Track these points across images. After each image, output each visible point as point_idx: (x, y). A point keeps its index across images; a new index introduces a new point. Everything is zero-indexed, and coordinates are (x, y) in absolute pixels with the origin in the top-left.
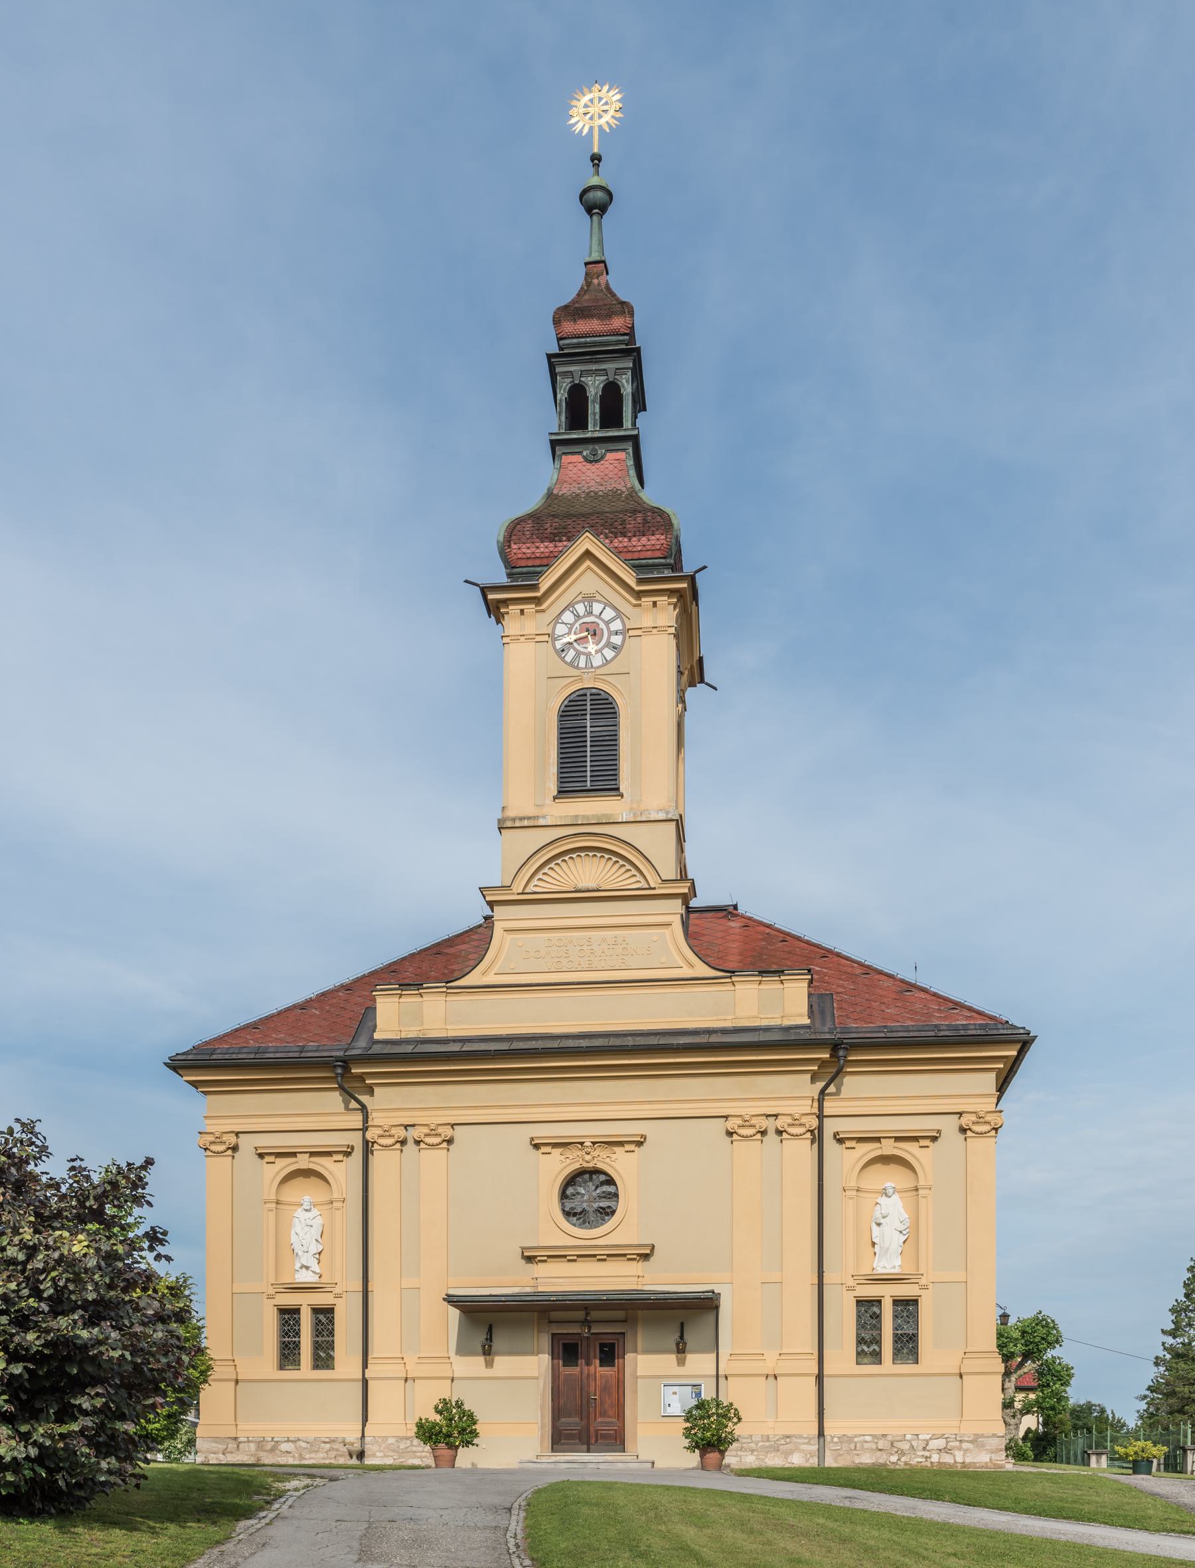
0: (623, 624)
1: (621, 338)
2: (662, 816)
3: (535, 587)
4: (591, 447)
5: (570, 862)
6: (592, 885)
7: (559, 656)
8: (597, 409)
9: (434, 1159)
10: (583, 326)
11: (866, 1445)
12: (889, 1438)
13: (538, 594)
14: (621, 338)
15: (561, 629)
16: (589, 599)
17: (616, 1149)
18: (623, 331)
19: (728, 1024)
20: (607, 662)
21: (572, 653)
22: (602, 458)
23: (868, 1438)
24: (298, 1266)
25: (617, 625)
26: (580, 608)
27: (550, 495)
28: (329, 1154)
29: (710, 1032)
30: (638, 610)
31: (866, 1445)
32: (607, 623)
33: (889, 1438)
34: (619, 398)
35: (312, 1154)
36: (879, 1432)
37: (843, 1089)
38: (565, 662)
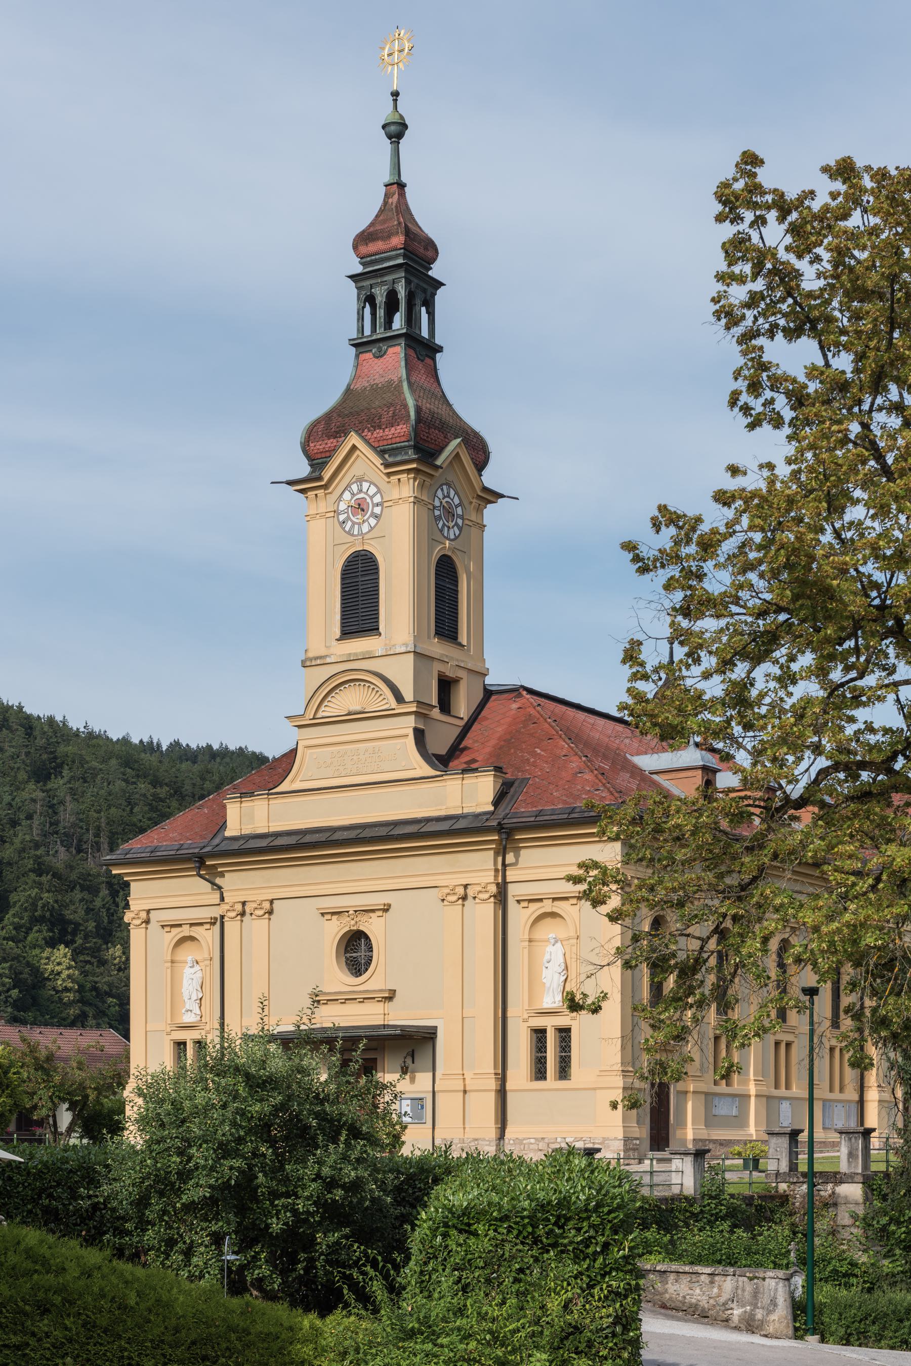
0: (382, 498)
1: (399, 252)
2: (403, 649)
3: (320, 478)
4: (377, 345)
5: (336, 696)
6: (358, 708)
7: (341, 526)
8: (382, 314)
9: (257, 927)
10: (373, 247)
11: (532, 1147)
12: (546, 1140)
13: (323, 483)
14: (399, 252)
15: (343, 506)
16: (360, 480)
17: (371, 914)
18: (399, 246)
19: (442, 813)
20: (372, 528)
21: (349, 524)
22: (385, 352)
23: (532, 1141)
24: (183, 1011)
25: (377, 499)
26: (355, 488)
27: (348, 391)
28: (201, 924)
29: (428, 820)
30: (390, 485)
31: (532, 1147)
32: (372, 497)
33: (546, 1140)
34: (397, 302)
35: (192, 925)
36: (540, 1136)
37: (520, 859)
38: (345, 531)
